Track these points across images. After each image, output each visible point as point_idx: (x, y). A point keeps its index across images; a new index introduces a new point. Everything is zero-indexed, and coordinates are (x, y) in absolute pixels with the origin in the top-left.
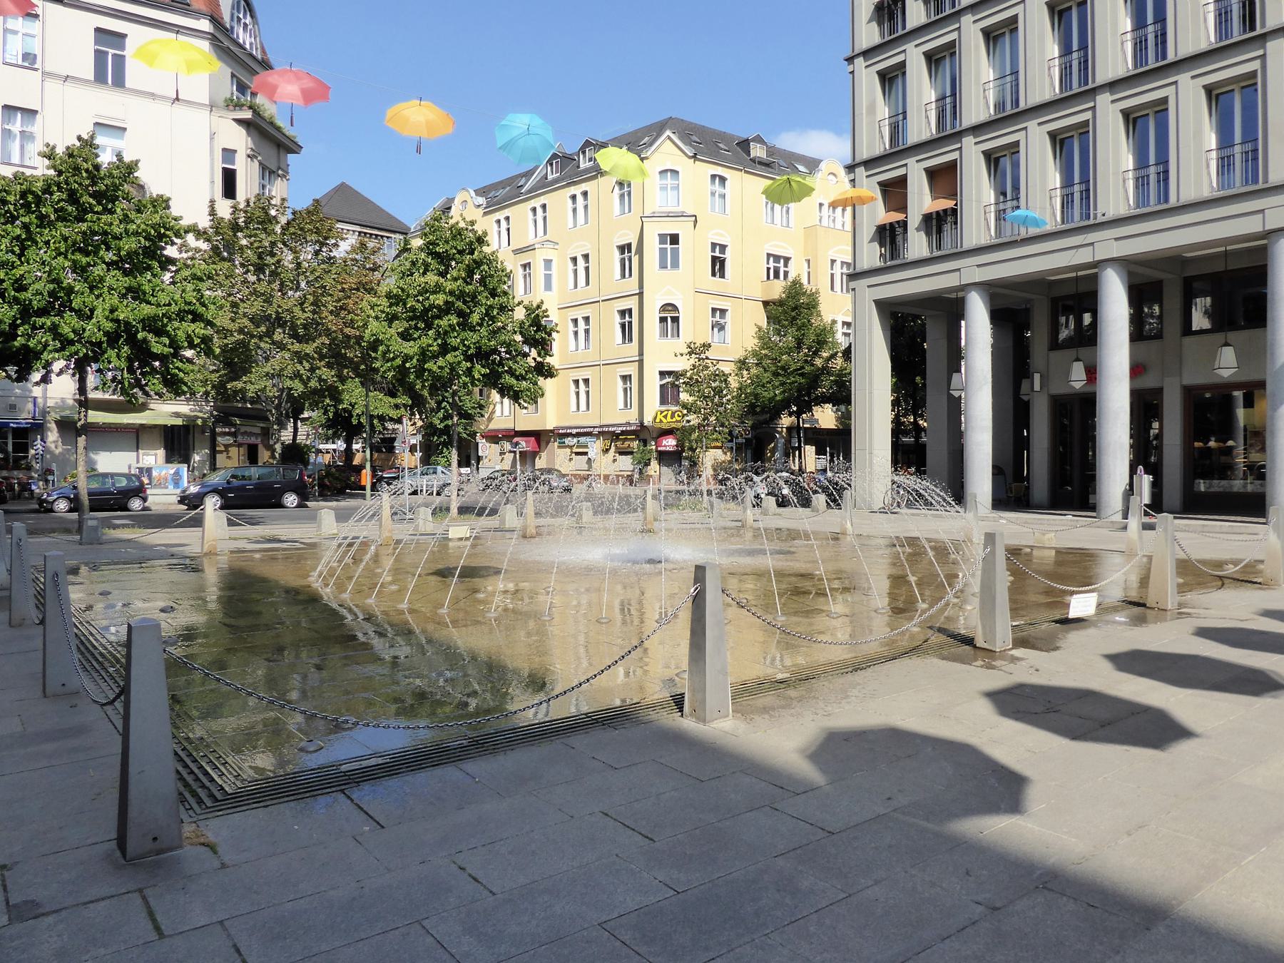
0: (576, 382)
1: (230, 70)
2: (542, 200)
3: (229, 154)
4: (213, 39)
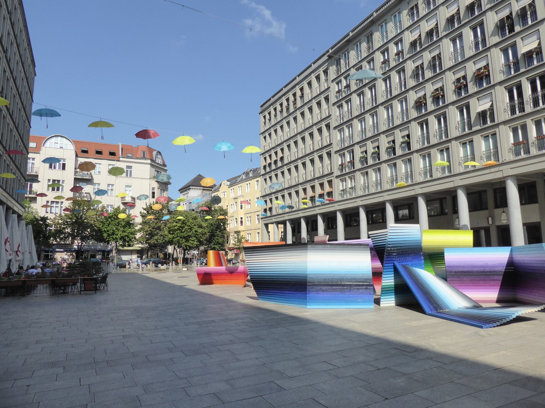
0: (248, 234)
1: (154, 169)
2: (241, 185)
3: (153, 189)
4: (151, 165)
